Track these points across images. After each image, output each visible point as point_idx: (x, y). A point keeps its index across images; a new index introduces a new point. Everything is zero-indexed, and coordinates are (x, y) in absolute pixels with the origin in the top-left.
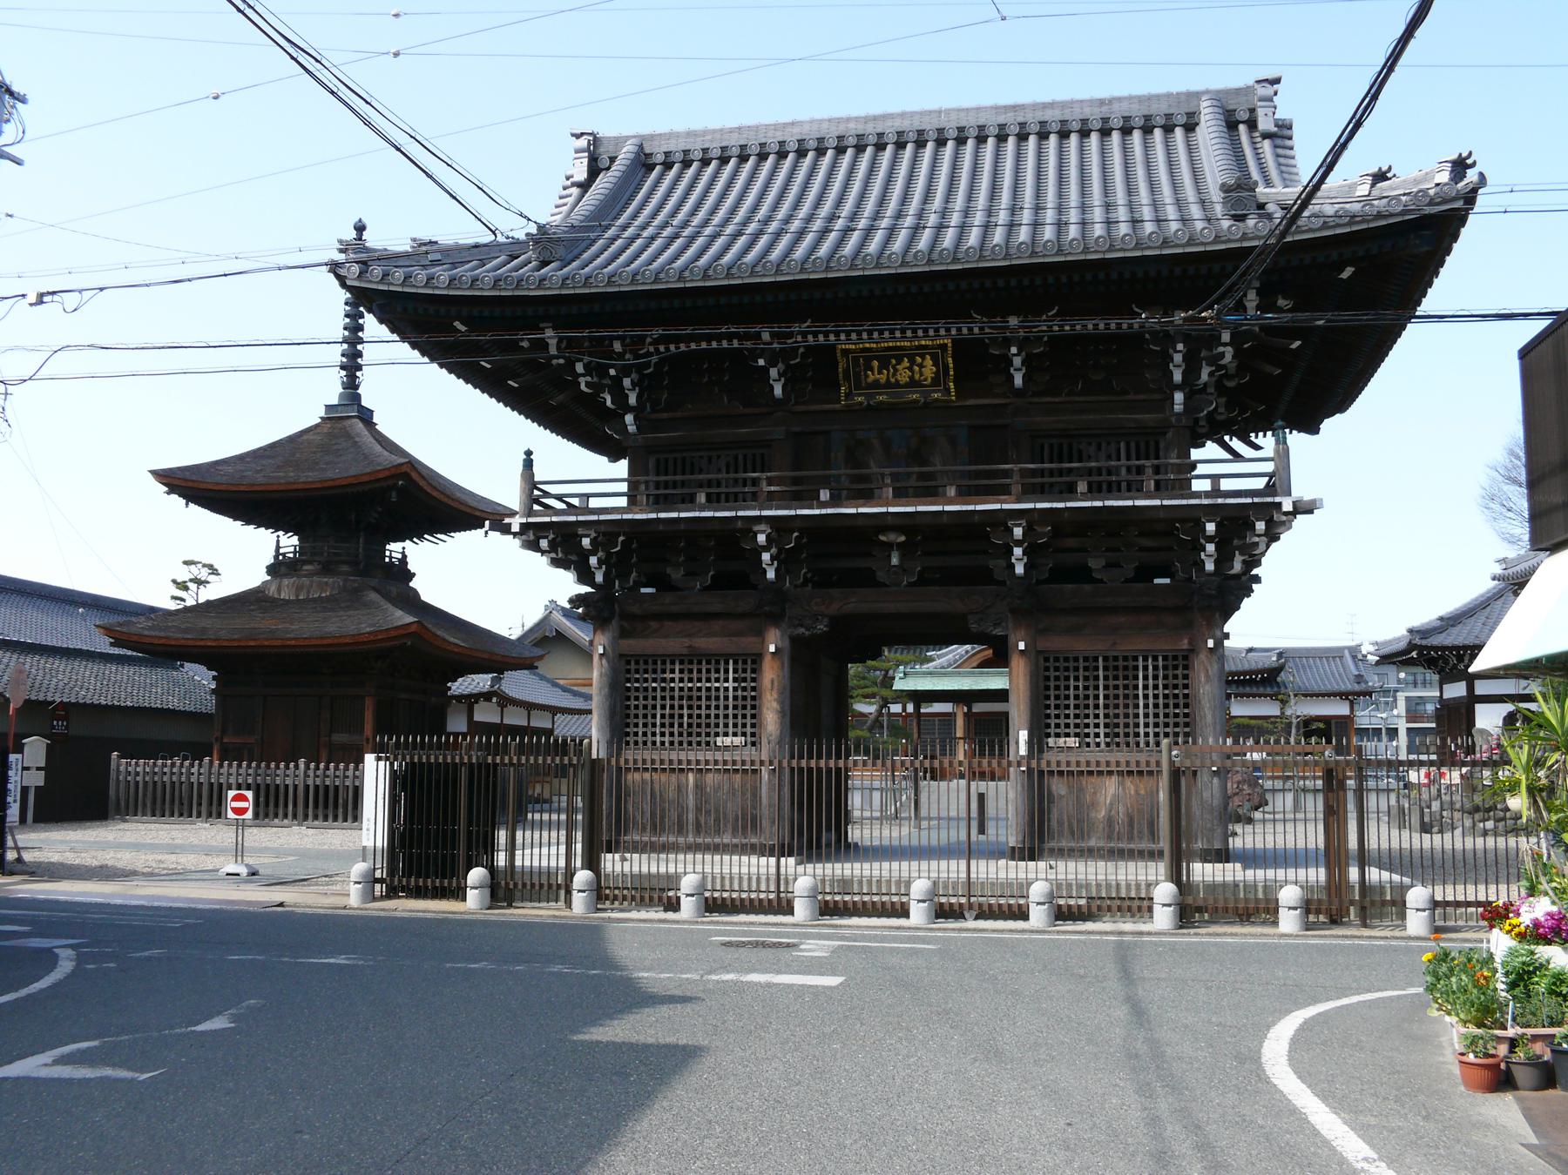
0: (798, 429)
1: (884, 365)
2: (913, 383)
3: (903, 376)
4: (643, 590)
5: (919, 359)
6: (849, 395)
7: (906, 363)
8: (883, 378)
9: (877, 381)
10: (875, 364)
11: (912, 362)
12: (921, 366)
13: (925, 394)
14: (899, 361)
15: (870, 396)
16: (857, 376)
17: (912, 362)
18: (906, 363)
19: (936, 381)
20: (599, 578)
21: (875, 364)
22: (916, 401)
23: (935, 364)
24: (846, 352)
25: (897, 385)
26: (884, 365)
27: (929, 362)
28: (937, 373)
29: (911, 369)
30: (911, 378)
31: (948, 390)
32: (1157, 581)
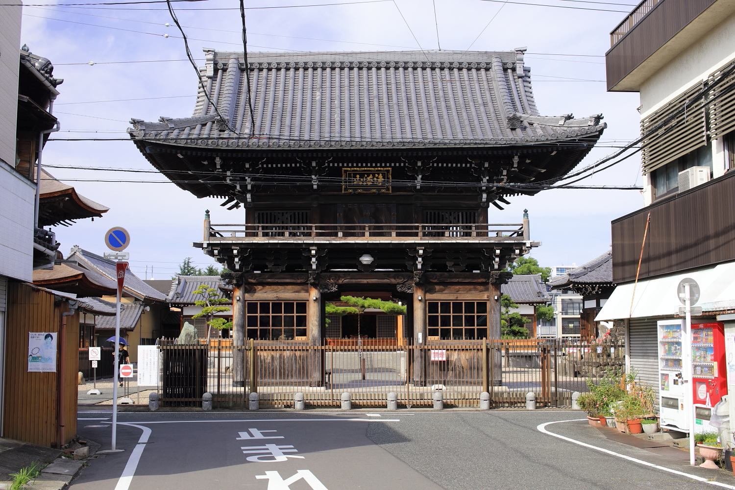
0: (322, 202)
1: (362, 176)
2: (373, 185)
4: (255, 272)
5: (377, 175)
6: (346, 189)
7: (371, 176)
10: (358, 176)
13: (379, 190)
14: (368, 176)
15: (355, 190)
17: (374, 176)
18: (371, 176)
20: (237, 267)
21: (358, 176)
22: (374, 193)
23: (384, 177)
24: (346, 171)
26: (362, 176)
27: (381, 176)
31: (388, 189)
32: (474, 271)
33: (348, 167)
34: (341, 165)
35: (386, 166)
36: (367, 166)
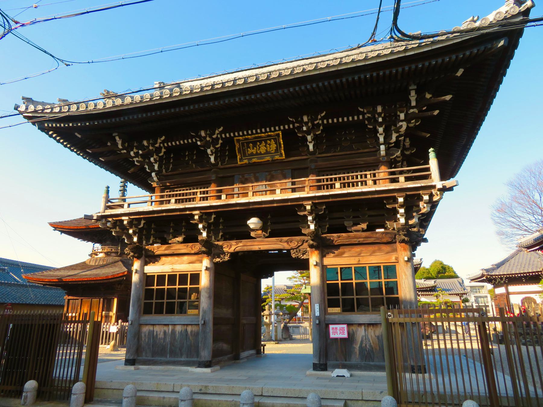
0: (221, 175)
2: (267, 153)
3: (263, 150)
5: (269, 142)
6: (241, 160)
7: (263, 143)
8: (254, 151)
9: (252, 153)
11: (266, 143)
12: (270, 145)
15: (249, 159)
16: (244, 151)
17: (266, 143)
18: (263, 143)
19: (277, 150)
23: (276, 143)
25: (261, 154)
28: (277, 147)
29: (265, 146)
30: (266, 150)
33: (239, 136)
34: (232, 135)
35: (275, 130)
36: (257, 133)
